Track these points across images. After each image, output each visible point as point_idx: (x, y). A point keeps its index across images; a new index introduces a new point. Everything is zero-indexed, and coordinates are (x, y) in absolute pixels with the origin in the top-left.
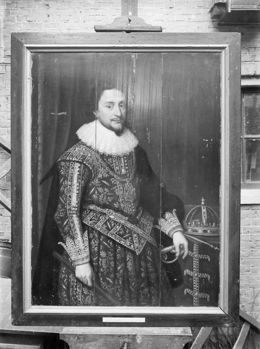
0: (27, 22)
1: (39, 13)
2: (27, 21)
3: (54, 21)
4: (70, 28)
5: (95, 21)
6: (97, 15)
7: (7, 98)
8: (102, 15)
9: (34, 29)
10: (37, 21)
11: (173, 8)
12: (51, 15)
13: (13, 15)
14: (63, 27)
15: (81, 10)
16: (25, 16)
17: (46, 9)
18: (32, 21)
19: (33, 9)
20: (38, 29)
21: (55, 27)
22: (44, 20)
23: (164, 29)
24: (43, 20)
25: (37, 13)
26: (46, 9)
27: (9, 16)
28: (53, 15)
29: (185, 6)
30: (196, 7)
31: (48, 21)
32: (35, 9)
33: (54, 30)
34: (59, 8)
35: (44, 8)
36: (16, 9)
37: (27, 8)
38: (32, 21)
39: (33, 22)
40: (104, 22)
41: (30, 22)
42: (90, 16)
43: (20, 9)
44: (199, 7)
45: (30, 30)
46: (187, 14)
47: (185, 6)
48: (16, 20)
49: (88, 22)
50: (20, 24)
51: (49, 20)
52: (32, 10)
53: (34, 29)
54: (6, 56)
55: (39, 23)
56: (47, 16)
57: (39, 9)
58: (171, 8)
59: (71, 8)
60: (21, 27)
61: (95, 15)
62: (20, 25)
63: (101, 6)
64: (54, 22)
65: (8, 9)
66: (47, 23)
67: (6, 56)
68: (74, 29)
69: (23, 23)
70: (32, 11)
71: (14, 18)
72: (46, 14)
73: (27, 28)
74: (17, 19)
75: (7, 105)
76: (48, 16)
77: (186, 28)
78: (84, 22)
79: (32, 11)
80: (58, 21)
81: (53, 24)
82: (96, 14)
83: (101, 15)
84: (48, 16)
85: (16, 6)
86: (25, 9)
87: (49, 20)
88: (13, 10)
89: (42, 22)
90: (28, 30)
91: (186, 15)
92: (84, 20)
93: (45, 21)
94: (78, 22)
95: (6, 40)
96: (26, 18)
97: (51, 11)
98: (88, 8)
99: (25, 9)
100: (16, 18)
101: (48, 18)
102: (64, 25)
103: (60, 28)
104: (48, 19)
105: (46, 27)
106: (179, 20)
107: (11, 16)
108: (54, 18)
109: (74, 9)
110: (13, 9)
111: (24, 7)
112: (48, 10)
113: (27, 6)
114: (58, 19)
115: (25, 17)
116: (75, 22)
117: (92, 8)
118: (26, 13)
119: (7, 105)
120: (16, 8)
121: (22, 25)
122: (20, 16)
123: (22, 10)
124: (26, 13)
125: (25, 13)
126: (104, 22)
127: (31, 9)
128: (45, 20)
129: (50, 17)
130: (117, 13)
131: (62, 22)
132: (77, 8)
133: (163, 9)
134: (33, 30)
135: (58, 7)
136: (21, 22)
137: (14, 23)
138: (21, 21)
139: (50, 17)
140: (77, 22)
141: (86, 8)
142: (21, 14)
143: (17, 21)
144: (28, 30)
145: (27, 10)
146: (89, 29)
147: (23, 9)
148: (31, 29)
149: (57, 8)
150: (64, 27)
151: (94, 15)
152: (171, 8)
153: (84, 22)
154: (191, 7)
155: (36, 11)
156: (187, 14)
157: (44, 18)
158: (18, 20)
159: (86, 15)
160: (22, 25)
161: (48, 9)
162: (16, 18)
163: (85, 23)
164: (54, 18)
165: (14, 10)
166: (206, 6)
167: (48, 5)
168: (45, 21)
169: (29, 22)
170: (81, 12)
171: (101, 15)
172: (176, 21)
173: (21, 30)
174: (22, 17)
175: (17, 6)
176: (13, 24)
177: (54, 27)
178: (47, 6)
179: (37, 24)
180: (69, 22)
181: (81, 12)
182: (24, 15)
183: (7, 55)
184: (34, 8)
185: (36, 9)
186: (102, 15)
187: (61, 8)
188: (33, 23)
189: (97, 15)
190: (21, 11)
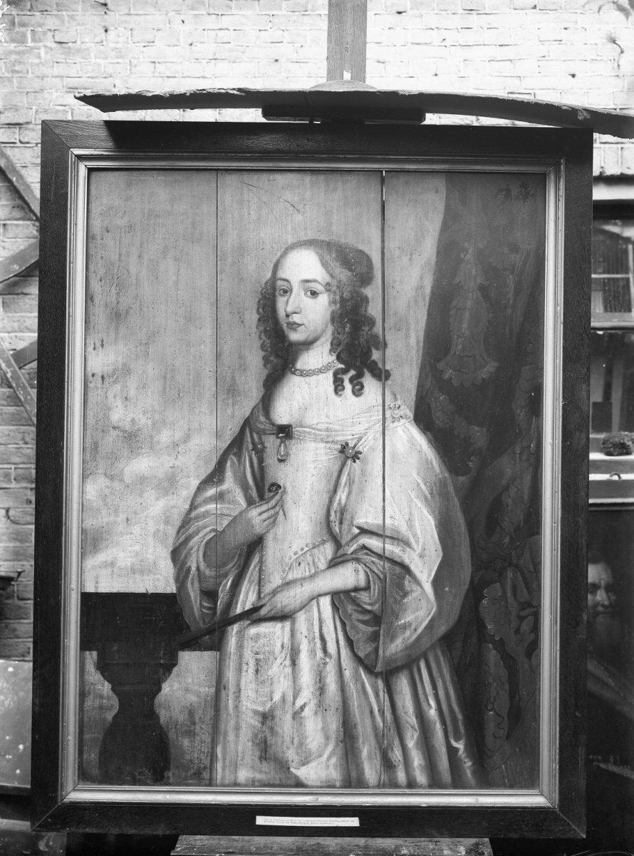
0: (55, 45)
1: (83, 24)
2: (56, 42)
3: (118, 43)
4: (156, 61)
5: (216, 42)
6: (221, 29)
7: (4, 225)
8: (234, 30)
9: (71, 61)
10: (79, 43)
11: (402, 14)
12: (113, 28)
13: (21, 29)
14: (141, 57)
15: (183, 17)
16: (50, 30)
17: (100, 15)
18: (67, 43)
19: (68, 13)
20: (81, 60)
21: (121, 57)
22: (95, 41)
23: (383, 63)
24: (94, 38)
25: (78, 24)
26: (100, 15)
27: (13, 29)
28: (116, 28)
29: (434, 10)
30: (461, 11)
31: (104, 43)
32: (74, 13)
33: (118, 63)
34: (132, 12)
35: (94, 13)
36: (31, 14)
37: (56, 13)
38: (67, 43)
39: (70, 44)
40: (239, 46)
41: (64, 45)
42: (206, 32)
43: (37, 14)
44: (468, 12)
45: (62, 63)
46: (437, 28)
47: (434, 10)
48: (29, 40)
49: (199, 45)
50: (39, 49)
51: (106, 40)
52: (68, 15)
53: (71, 61)
54: (3, 125)
55: (84, 46)
56: (103, 31)
57: (84, 15)
58: (399, 13)
59: (160, 13)
60: (40, 58)
61: (218, 28)
62: (37, 51)
63: (231, 8)
64: (119, 45)
65: (11, 15)
66: (102, 47)
67: (5, 126)
68: (166, 62)
69: (45, 47)
70: (66, 18)
71: (24, 35)
72: (100, 25)
73: (55, 60)
74: (32, 38)
75: (4, 242)
76: (106, 31)
77: (435, 60)
78: (191, 44)
79: (66, 18)
80: (128, 43)
81: (117, 49)
82: (220, 27)
83: (231, 28)
84: (106, 31)
85: (29, 7)
86: (50, 13)
87: (106, 40)
88: (23, 17)
89: (89, 45)
90: (57, 63)
91: (436, 30)
92: (190, 42)
93: (97, 43)
94: (177, 45)
95: (4, 86)
96: (54, 36)
97: (112, 18)
98: (200, 12)
99: (50, 13)
100: (29, 35)
101: (106, 37)
102: (143, 52)
103: (132, 61)
104: (104, 38)
105: (101, 58)
106: (420, 42)
107: (17, 29)
108: (119, 36)
109: (167, 14)
110: (22, 13)
111: (49, 9)
112: (106, 17)
113: (55, 6)
114: (128, 38)
115: (50, 34)
116: (169, 46)
117: (212, 12)
118: (54, 23)
119: (4, 242)
120: (30, 11)
121: (42, 51)
122: (40, 29)
123: (44, 16)
124: (54, 23)
125: (51, 22)
126: (239, 46)
127: (64, 13)
128: (98, 39)
129: (112, 34)
130: (270, 25)
131: (139, 44)
132: (174, 13)
133: (380, 14)
134: (67, 63)
135: (130, 10)
136: (41, 44)
137: (26, 46)
138: (40, 41)
139: (109, 32)
140: (174, 46)
141: (196, 12)
142: (40, 25)
143: (31, 42)
144: (57, 63)
145: (57, 15)
146: (203, 61)
147: (46, 13)
148: (64, 61)
149: (127, 12)
150: (144, 58)
151: (215, 28)
152: (399, 13)
153: (191, 44)
154: (448, 12)
155: (77, 18)
156: (437, 28)
157: (95, 36)
158: (34, 40)
159: (196, 29)
160: (42, 51)
161: (105, 13)
162: (29, 35)
163: (192, 46)
164: (119, 36)
165: (24, 15)
166: (485, 8)
167: (105, 5)
168: (97, 43)
169: (59, 46)
170: (183, 22)
171: (231, 28)
172: (412, 43)
173: (41, 63)
174: (44, 33)
175: (31, 6)
176: (25, 48)
177: (118, 57)
178: (104, 7)
179: (78, 51)
180: (155, 46)
181: (183, 22)
182: (49, 28)
183: (7, 122)
184: (73, 11)
185: (77, 15)
186: (234, 30)
187: (135, 13)
188: (69, 48)
189: (221, 29)
190: (41, 18)
